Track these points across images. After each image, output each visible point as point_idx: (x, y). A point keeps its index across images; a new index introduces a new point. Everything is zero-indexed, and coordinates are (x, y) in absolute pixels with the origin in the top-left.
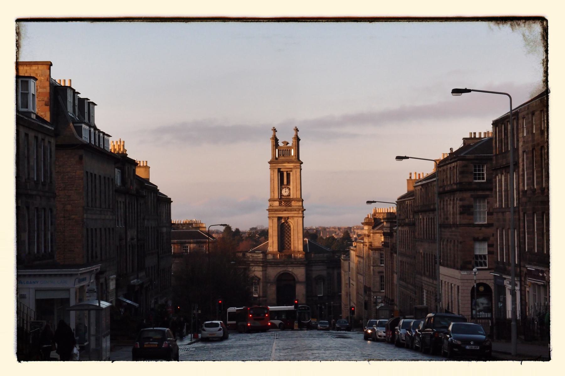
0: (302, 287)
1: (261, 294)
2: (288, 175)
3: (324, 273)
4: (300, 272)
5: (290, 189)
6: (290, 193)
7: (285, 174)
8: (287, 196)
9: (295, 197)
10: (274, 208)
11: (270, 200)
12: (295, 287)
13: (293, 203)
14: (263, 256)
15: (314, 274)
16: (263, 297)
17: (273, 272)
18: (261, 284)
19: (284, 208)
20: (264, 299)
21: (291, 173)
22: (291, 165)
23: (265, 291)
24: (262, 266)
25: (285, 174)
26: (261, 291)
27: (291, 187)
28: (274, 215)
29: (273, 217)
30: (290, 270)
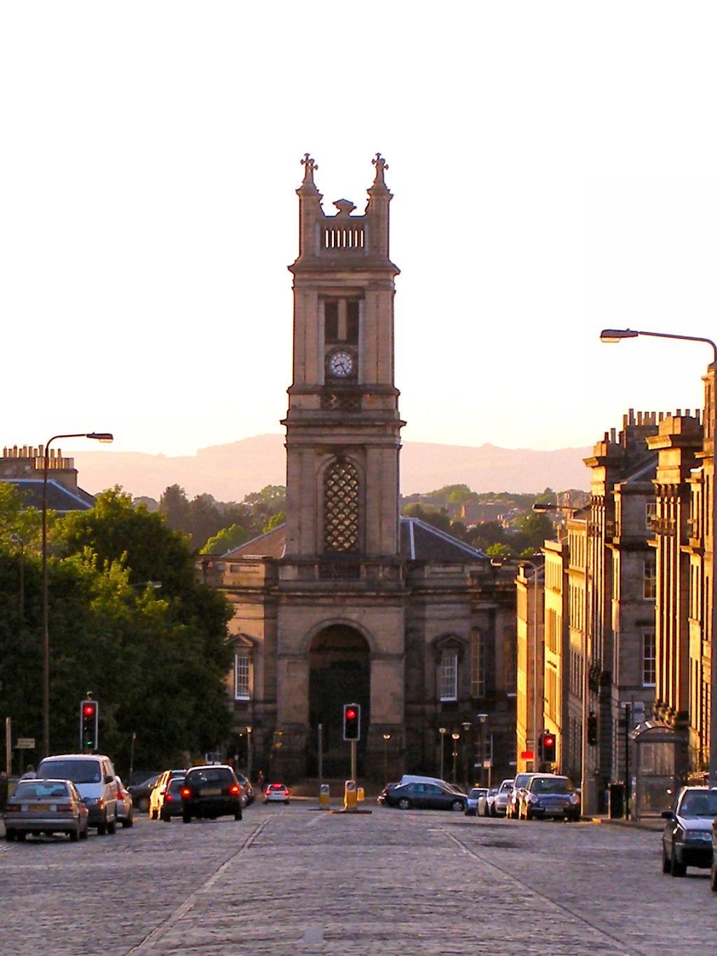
0: (392, 670)
1: (261, 696)
3: (462, 628)
4: (383, 625)
5: (355, 357)
6: (355, 367)
7: (342, 306)
9: (374, 381)
10: (304, 415)
12: (367, 673)
13: (367, 402)
14: (267, 570)
15: (431, 632)
16: (266, 701)
17: (300, 624)
19: (336, 415)
20: (270, 706)
22: (360, 279)
23: (271, 684)
24: (265, 603)
25: (342, 306)
28: (306, 440)
29: (301, 445)
30: (354, 616)
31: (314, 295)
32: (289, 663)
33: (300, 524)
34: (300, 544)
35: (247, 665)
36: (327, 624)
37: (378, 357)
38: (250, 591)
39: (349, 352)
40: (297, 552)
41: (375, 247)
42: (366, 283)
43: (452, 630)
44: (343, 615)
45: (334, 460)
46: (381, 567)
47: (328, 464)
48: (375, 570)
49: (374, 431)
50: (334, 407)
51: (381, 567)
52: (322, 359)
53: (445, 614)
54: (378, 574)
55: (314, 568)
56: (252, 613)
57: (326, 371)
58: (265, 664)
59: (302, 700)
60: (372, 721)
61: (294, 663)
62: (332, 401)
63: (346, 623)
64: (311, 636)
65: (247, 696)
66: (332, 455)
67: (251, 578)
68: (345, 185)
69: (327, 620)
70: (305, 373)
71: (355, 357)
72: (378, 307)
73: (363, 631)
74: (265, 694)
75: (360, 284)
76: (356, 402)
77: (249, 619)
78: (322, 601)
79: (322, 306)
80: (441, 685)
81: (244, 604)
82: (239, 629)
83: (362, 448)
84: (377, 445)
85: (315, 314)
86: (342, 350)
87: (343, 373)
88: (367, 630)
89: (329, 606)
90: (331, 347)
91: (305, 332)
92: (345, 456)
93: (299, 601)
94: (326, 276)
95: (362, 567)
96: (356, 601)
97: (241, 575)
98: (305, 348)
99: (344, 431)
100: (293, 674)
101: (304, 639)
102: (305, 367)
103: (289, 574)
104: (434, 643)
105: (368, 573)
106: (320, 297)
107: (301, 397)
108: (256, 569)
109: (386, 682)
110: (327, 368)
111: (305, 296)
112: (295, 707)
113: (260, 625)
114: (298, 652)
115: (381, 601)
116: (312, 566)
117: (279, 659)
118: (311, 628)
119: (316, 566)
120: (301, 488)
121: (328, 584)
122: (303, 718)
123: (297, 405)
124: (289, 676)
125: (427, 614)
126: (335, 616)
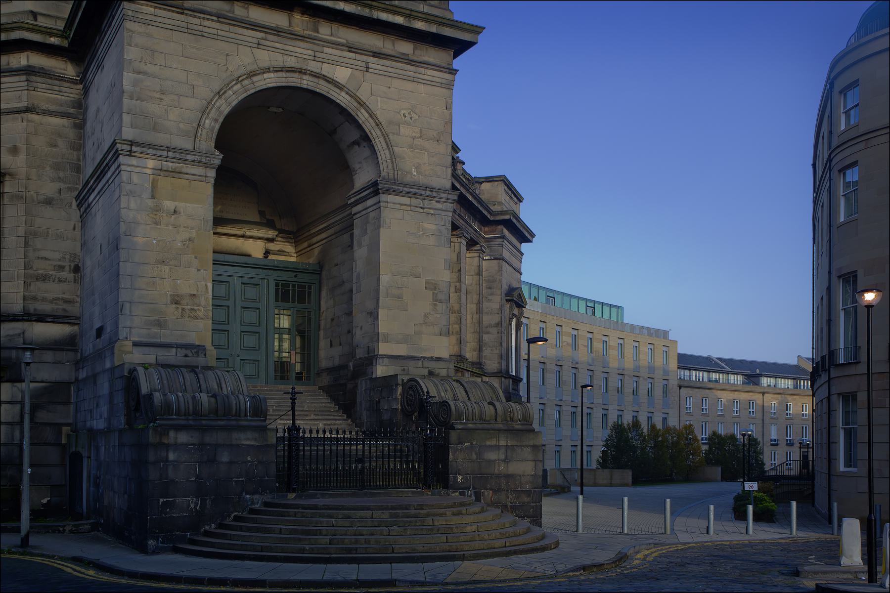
44: (313, 66)
63: (322, 87)
69: (268, 70)
100: (169, 205)
101: (204, 112)
112: (176, 301)
117: (131, 154)
118: (228, 86)
124: (157, 209)
126: (291, 62)
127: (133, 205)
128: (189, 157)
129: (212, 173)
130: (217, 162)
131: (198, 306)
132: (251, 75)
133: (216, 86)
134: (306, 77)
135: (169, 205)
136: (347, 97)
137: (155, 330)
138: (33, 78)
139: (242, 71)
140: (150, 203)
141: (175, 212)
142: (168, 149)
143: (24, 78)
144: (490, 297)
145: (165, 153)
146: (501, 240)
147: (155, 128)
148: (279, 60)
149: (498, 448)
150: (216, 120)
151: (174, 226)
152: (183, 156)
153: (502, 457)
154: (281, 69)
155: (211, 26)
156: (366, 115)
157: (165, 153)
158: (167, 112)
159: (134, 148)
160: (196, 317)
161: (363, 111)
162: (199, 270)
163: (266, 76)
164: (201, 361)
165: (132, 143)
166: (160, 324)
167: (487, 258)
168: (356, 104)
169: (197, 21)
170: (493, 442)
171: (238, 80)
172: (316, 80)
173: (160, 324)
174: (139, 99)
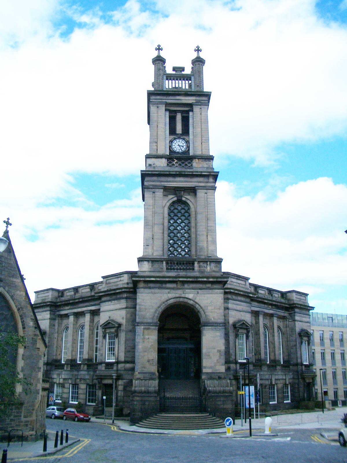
1: (122, 358)
2: (186, 121)
3: (248, 318)
4: (209, 303)
5: (187, 142)
6: (188, 147)
7: (179, 117)
8: (183, 153)
11: (148, 157)
16: (126, 362)
17: (151, 302)
18: (123, 336)
20: (128, 366)
21: (191, 113)
25: (179, 117)
26: (122, 348)
27: (191, 136)
28: (158, 183)
30: (191, 296)
31: (163, 108)
32: (144, 329)
33: (153, 235)
34: (153, 248)
35: (114, 339)
36: (172, 301)
37: (202, 140)
38: (117, 291)
39: (184, 139)
40: (150, 254)
41: (198, 86)
42: (194, 101)
43: (243, 318)
44: (183, 295)
45: (175, 199)
46: (209, 263)
47: (171, 202)
48: (205, 265)
49: (201, 179)
50: (175, 166)
51: (209, 263)
52: (168, 142)
53: (239, 308)
54: (207, 268)
55: (163, 264)
56: (118, 306)
57: (170, 149)
58: (126, 337)
59: (154, 355)
60: (204, 370)
61: (148, 329)
62: (174, 163)
63: (186, 300)
64: (160, 310)
65: (113, 359)
66: (174, 196)
67: (117, 285)
68: (179, 58)
69: (171, 299)
70: (157, 147)
71: (187, 142)
72: (201, 114)
73: (197, 306)
74: (125, 357)
75: (190, 102)
76: (189, 163)
77: (116, 310)
78: (168, 285)
79: (168, 116)
80: (238, 352)
81: (113, 302)
82: (110, 317)
83: (193, 191)
84: (204, 188)
85: (164, 117)
86: (179, 138)
87: (180, 150)
88: (199, 305)
89: (173, 289)
90: (172, 137)
91: (157, 126)
92: (182, 197)
93: (152, 285)
94: (171, 98)
95: (196, 264)
96: (192, 286)
97: (112, 284)
98: (157, 134)
99: (182, 179)
100: (147, 337)
101: (155, 312)
102: (157, 144)
103: (146, 266)
104: (234, 326)
105: (199, 267)
106: (166, 110)
107: (153, 160)
108: (122, 278)
109: (212, 342)
110: (170, 147)
111: (158, 107)
112: (149, 361)
113: (123, 313)
114: (150, 321)
115: (209, 285)
116: (162, 261)
117: (138, 325)
118: (161, 305)
119: (164, 263)
120: (154, 213)
121: (173, 274)
122: (154, 369)
123: (152, 164)
124: (144, 338)
125: (230, 306)
126: (177, 295)
127: (139, 338)
128: (151, 324)
129: (157, 328)
130: (158, 325)
131: (154, 362)
132: (167, 301)
133: (158, 305)
134: (181, 299)
135: (147, 337)
136: (192, 302)
137: (143, 369)
138: (127, 300)
139: (165, 300)
140: (142, 337)
141: (148, 338)
142: (146, 323)
143: (125, 300)
144: (292, 335)
145: (145, 324)
146: (294, 314)
147: (144, 318)
148: (173, 295)
149: (220, 401)
150: (158, 314)
151: (148, 342)
152: (150, 324)
153: (222, 403)
154: (174, 298)
155: (157, 291)
156: (198, 306)
157: (145, 324)
158: (147, 314)
159: (139, 324)
160: (153, 365)
161: (197, 305)
162: (154, 353)
163: (171, 300)
164: (154, 377)
165: (138, 323)
166: (145, 368)
167: (290, 320)
168: (195, 303)
169: (154, 290)
170: (219, 399)
171: (164, 303)
172: (184, 299)
173: (145, 368)
174: (140, 311)
